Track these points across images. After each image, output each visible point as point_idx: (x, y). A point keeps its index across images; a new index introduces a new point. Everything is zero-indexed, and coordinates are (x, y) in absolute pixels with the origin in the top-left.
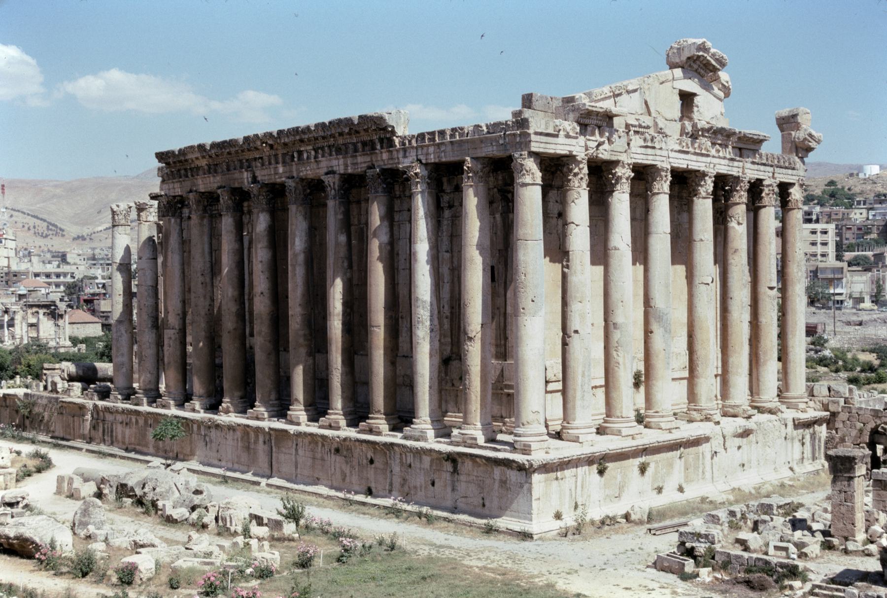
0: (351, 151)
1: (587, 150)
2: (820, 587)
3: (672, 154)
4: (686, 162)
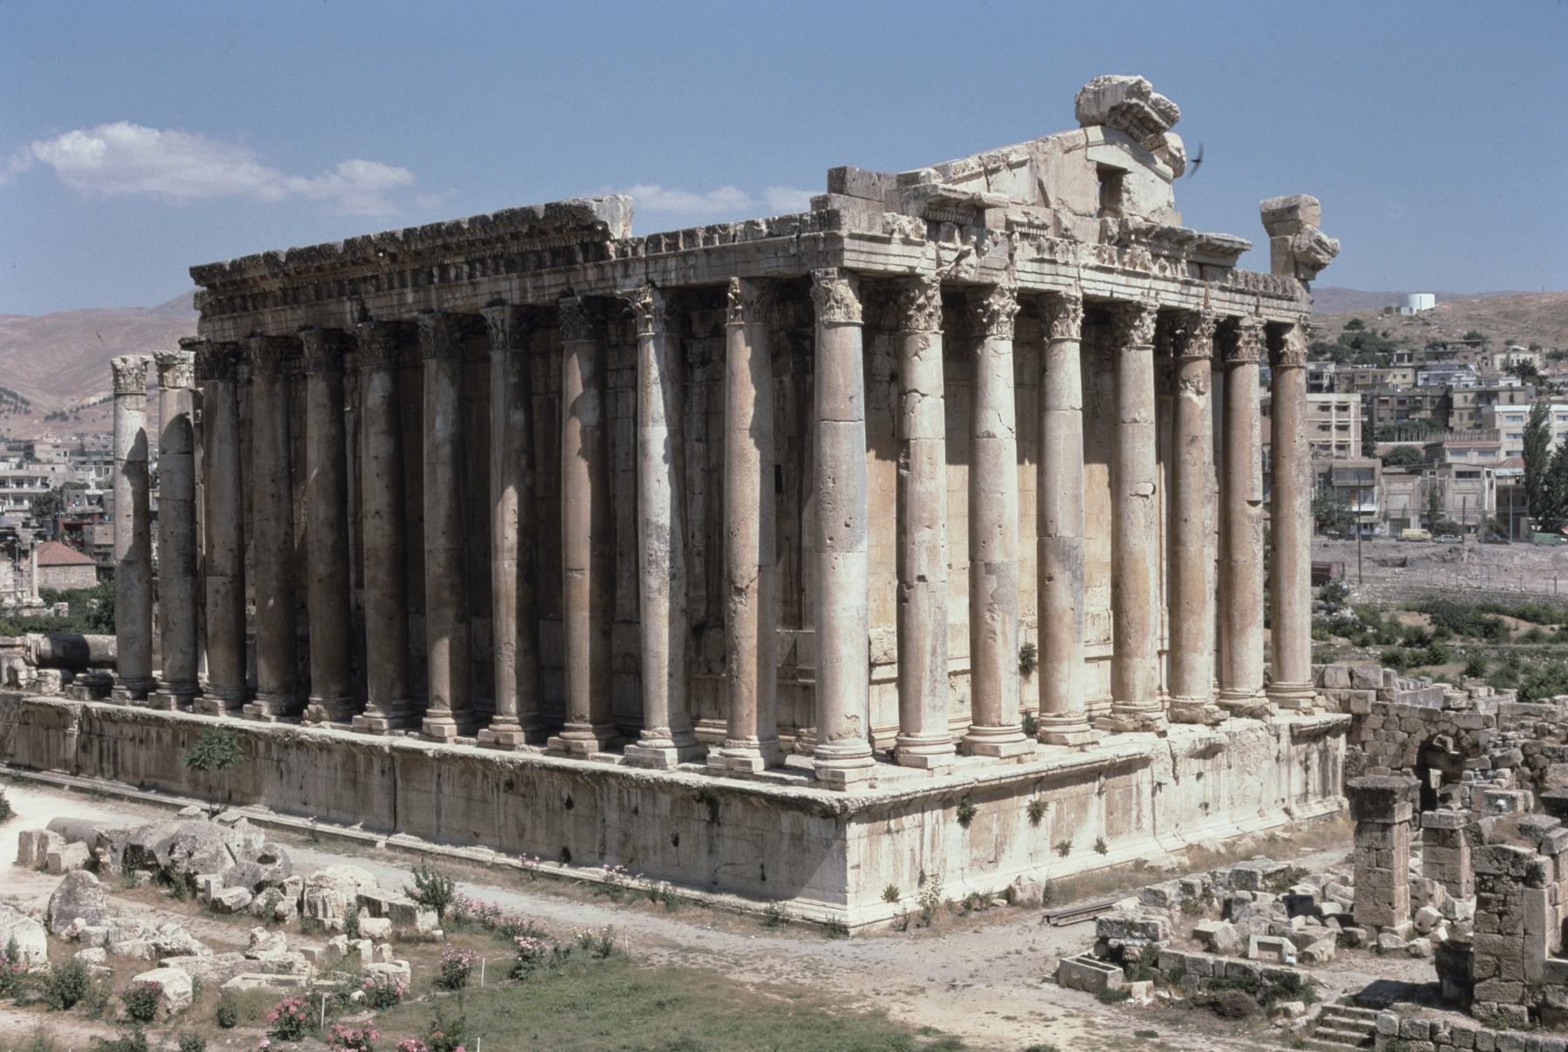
1: (939, 264)
2: (1335, 1011)
3: (1086, 274)
4: (1109, 287)
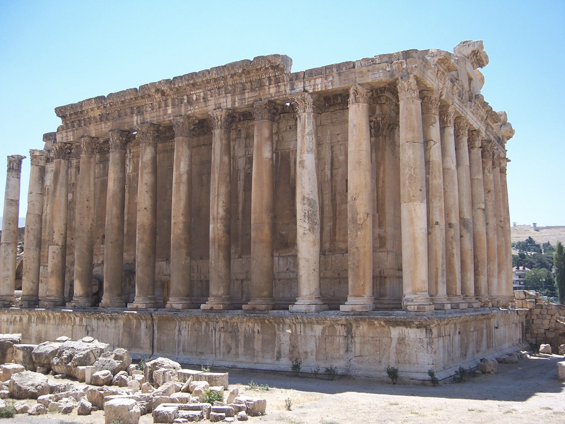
0: (238, 90)
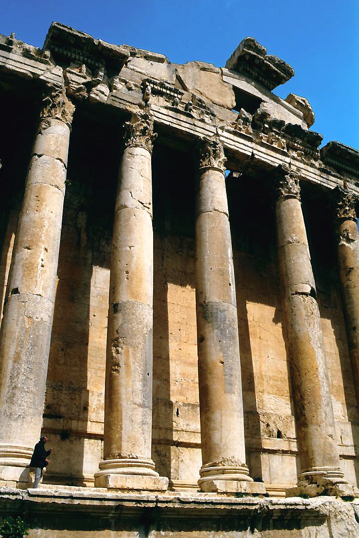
4: (251, 150)
